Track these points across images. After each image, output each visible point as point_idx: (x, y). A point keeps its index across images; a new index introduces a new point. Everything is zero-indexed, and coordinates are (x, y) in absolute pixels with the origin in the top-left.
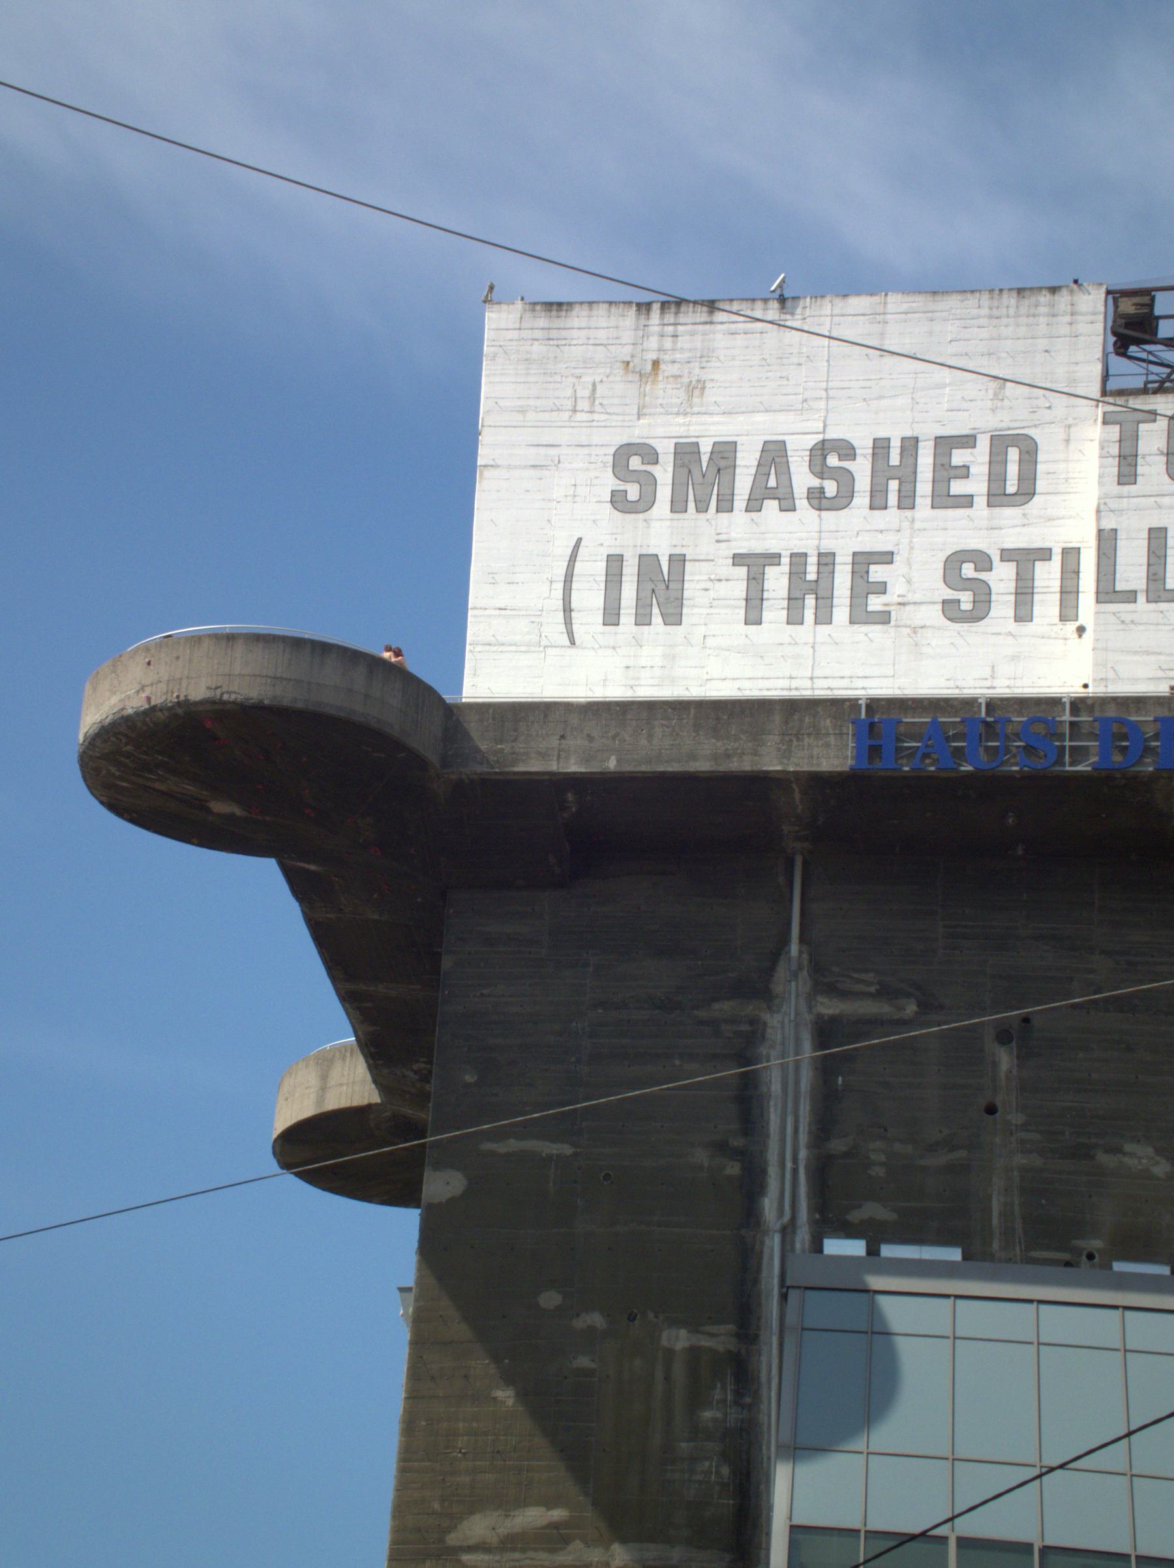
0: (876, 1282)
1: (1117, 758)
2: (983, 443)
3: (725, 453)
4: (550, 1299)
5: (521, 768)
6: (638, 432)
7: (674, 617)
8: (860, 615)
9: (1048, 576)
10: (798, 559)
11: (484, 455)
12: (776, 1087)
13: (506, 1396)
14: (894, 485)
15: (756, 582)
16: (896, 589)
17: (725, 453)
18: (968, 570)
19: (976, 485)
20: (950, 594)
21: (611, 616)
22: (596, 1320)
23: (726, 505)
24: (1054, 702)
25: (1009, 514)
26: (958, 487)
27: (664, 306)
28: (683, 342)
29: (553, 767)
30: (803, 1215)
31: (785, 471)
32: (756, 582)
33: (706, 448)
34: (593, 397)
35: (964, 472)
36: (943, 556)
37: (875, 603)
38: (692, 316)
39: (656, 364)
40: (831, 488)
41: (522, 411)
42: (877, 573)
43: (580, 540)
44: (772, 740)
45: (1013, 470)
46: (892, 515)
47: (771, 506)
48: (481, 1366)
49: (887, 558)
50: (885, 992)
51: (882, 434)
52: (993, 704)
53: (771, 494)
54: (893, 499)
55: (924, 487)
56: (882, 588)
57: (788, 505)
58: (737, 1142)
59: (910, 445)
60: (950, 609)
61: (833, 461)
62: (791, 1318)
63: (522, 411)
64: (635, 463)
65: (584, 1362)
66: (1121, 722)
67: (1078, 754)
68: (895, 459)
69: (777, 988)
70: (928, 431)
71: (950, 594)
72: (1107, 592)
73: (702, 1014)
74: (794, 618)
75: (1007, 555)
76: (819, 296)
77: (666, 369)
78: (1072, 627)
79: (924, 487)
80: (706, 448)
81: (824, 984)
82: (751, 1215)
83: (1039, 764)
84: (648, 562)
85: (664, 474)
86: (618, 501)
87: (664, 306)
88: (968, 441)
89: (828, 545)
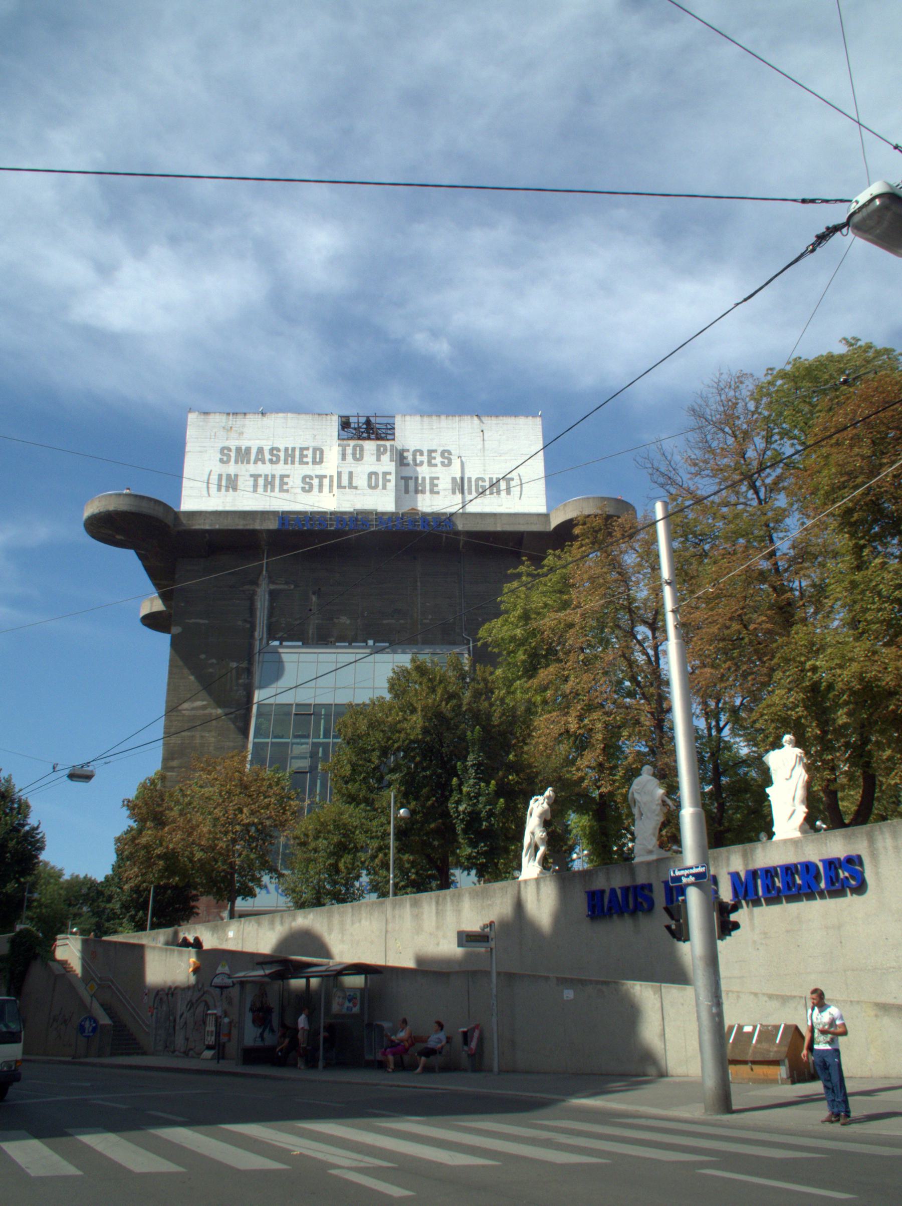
0: (281, 650)
1: (340, 526)
2: (311, 450)
3: (248, 450)
4: (203, 656)
5: (194, 528)
6: (226, 444)
7: (235, 489)
8: (282, 490)
9: (326, 482)
10: (266, 476)
11: (188, 448)
12: (259, 606)
13: (192, 678)
14: (290, 459)
15: (256, 481)
16: (291, 484)
17: (248, 450)
18: (308, 480)
19: (309, 459)
20: (303, 485)
21: (219, 489)
22: (214, 661)
23: (248, 462)
24: (326, 513)
25: (317, 467)
26: (305, 460)
27: (233, 414)
28: (238, 423)
29: (202, 527)
30: (265, 636)
31: (263, 454)
32: (256, 481)
33: (243, 448)
34: (215, 436)
35: (306, 456)
36: (301, 476)
37: (285, 487)
38: (239, 416)
39: (231, 428)
40: (274, 459)
41: (197, 438)
42: (286, 480)
43: (211, 471)
44: (258, 521)
45: (318, 456)
46: (289, 466)
47: (260, 463)
48: (186, 671)
49: (288, 476)
50: (287, 583)
51: (287, 446)
52: (312, 513)
53: (260, 460)
54: (289, 462)
55: (297, 459)
56: (287, 484)
57: (264, 462)
58: (249, 619)
59: (294, 449)
60: (303, 489)
61: (275, 452)
62: (261, 659)
63: (197, 438)
64: (226, 451)
65: (211, 670)
66: (341, 518)
67: (331, 525)
68: (290, 452)
69: (260, 582)
70: (298, 446)
71: (303, 485)
72: (340, 486)
73: (241, 589)
74: (265, 490)
75: (317, 476)
76: (271, 413)
77: (234, 429)
78: (332, 494)
79: (297, 459)
80: (243, 448)
81: (271, 581)
82: (252, 636)
83: (322, 528)
84: (229, 476)
85: (233, 454)
86: (221, 461)
87: (233, 414)
88: (307, 449)
89: (273, 473)
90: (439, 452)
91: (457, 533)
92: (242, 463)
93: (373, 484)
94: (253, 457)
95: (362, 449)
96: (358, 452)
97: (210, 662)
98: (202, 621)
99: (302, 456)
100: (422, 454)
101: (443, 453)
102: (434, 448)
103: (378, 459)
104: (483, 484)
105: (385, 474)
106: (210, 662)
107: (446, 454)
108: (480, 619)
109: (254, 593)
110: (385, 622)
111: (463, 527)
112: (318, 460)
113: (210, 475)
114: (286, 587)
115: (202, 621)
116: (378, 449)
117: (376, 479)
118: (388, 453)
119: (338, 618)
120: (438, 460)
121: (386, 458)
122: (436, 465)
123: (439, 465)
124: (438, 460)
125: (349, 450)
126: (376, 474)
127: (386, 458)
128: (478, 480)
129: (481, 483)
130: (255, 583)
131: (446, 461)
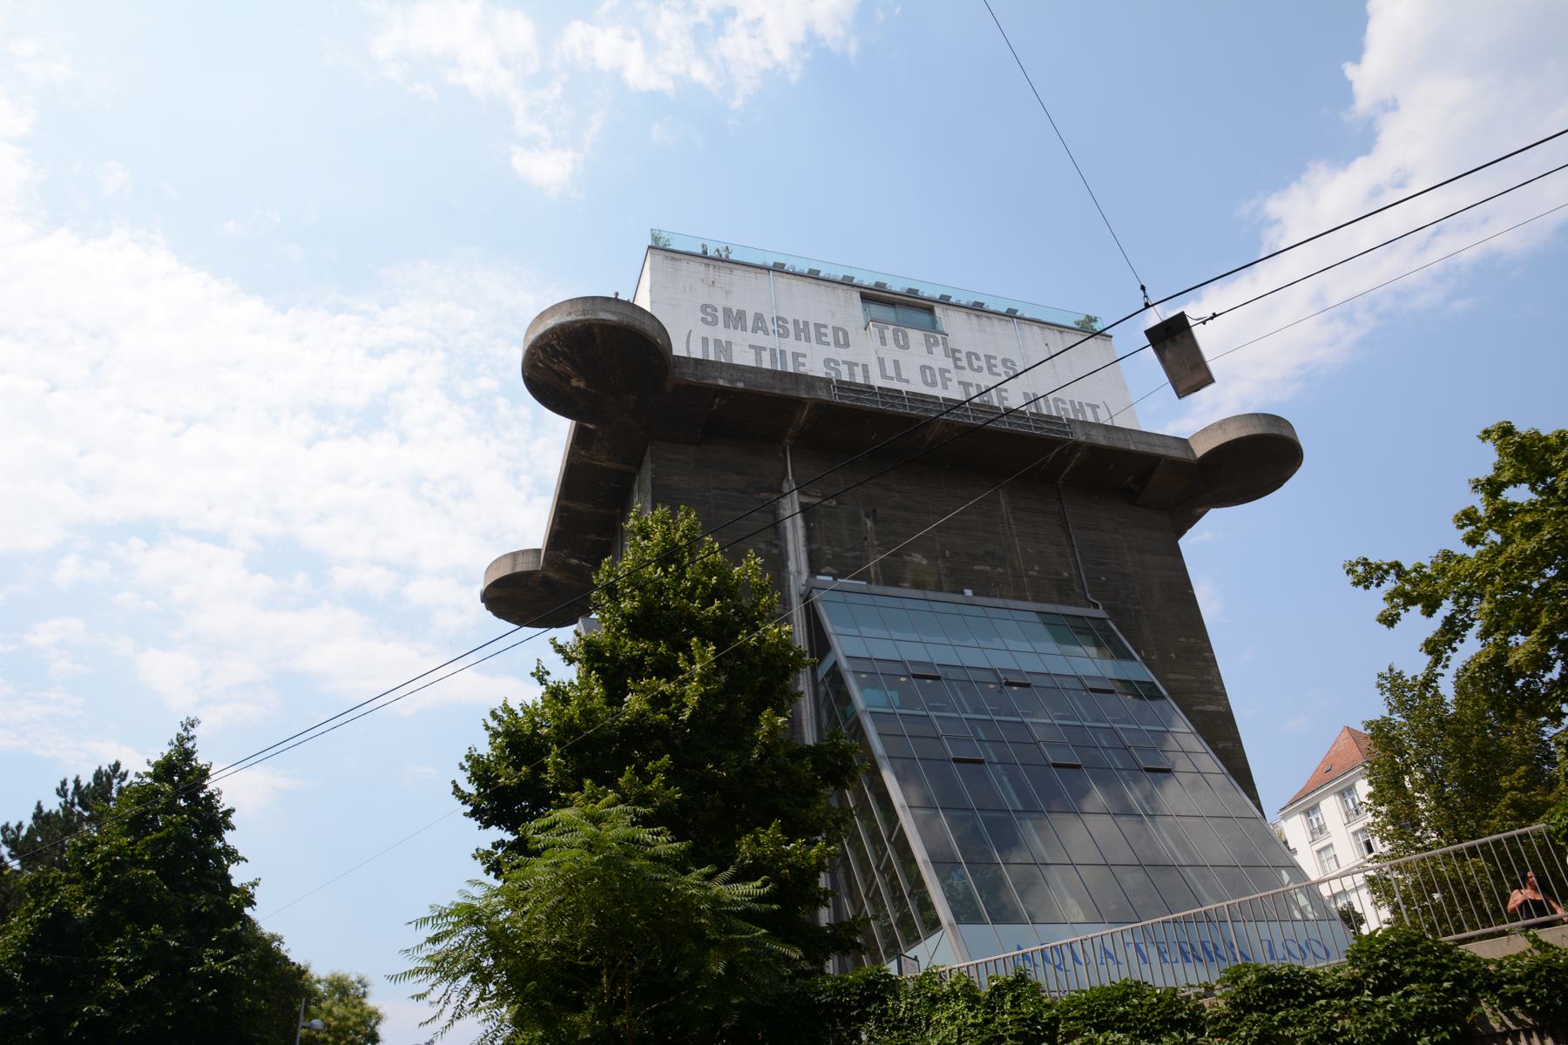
3: (741, 315)
6: (708, 302)
19: (830, 338)
26: (824, 339)
31: (763, 321)
34: (691, 288)
35: (826, 335)
39: (713, 282)
49: (804, 356)
53: (760, 329)
57: (766, 333)
73: (757, 496)
75: (844, 362)
85: (720, 315)
88: (825, 326)
90: (1000, 358)
92: (736, 328)
94: (750, 324)
95: (905, 336)
96: (901, 338)
99: (819, 335)
100: (978, 358)
102: (993, 354)
104: (1064, 406)
108: (1104, 579)
110: (976, 567)
113: (689, 336)
116: (927, 341)
117: (931, 374)
118: (941, 346)
119: (910, 555)
121: (939, 351)
125: (889, 333)
127: (939, 351)
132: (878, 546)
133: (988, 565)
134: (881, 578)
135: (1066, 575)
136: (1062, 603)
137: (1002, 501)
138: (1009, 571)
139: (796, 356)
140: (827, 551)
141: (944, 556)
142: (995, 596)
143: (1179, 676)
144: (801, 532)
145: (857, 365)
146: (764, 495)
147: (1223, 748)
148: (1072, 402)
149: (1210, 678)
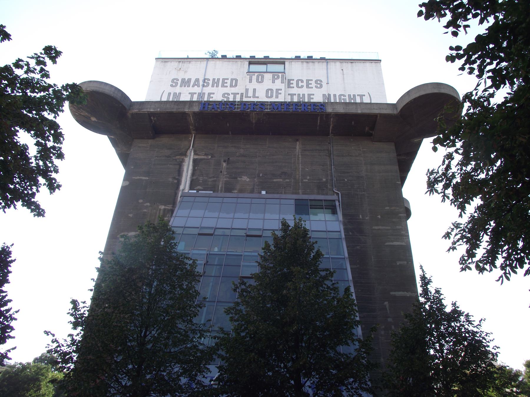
2: (230, 80)
3: (190, 80)
4: (141, 201)
17: (190, 80)
18: (226, 95)
19: (228, 84)
23: (189, 86)
34: (169, 73)
39: (180, 69)
40: (205, 84)
42: (212, 96)
49: (214, 94)
53: (196, 85)
58: (177, 177)
59: (218, 80)
61: (206, 81)
65: (145, 211)
68: (216, 81)
75: (232, 94)
77: (181, 69)
81: (195, 154)
85: (179, 82)
91: (328, 115)
93: (269, 95)
94: (192, 84)
97: (146, 205)
98: (144, 178)
101: (316, 82)
103: (273, 82)
105: (277, 90)
106: (146, 205)
107: (319, 82)
108: (346, 180)
109: (183, 161)
110: (275, 180)
111: (333, 110)
112: (234, 85)
114: (205, 157)
115: (144, 178)
118: (280, 79)
119: (242, 177)
120: (313, 84)
122: (312, 88)
123: (314, 88)
124: (313, 84)
126: (271, 90)
127: (278, 82)
128: (340, 95)
129: (342, 97)
130: (185, 155)
131: (319, 86)
132: (226, 174)
133: (282, 179)
134: (223, 189)
135: (324, 180)
136: (318, 194)
137: (298, 147)
138: (293, 180)
139: (309, 95)
140: (200, 179)
141: (259, 176)
142: (282, 193)
143: (381, 227)
144: (190, 172)
145: (238, 94)
146: (178, 157)
147: (400, 264)
148: (349, 96)
149: (401, 227)
